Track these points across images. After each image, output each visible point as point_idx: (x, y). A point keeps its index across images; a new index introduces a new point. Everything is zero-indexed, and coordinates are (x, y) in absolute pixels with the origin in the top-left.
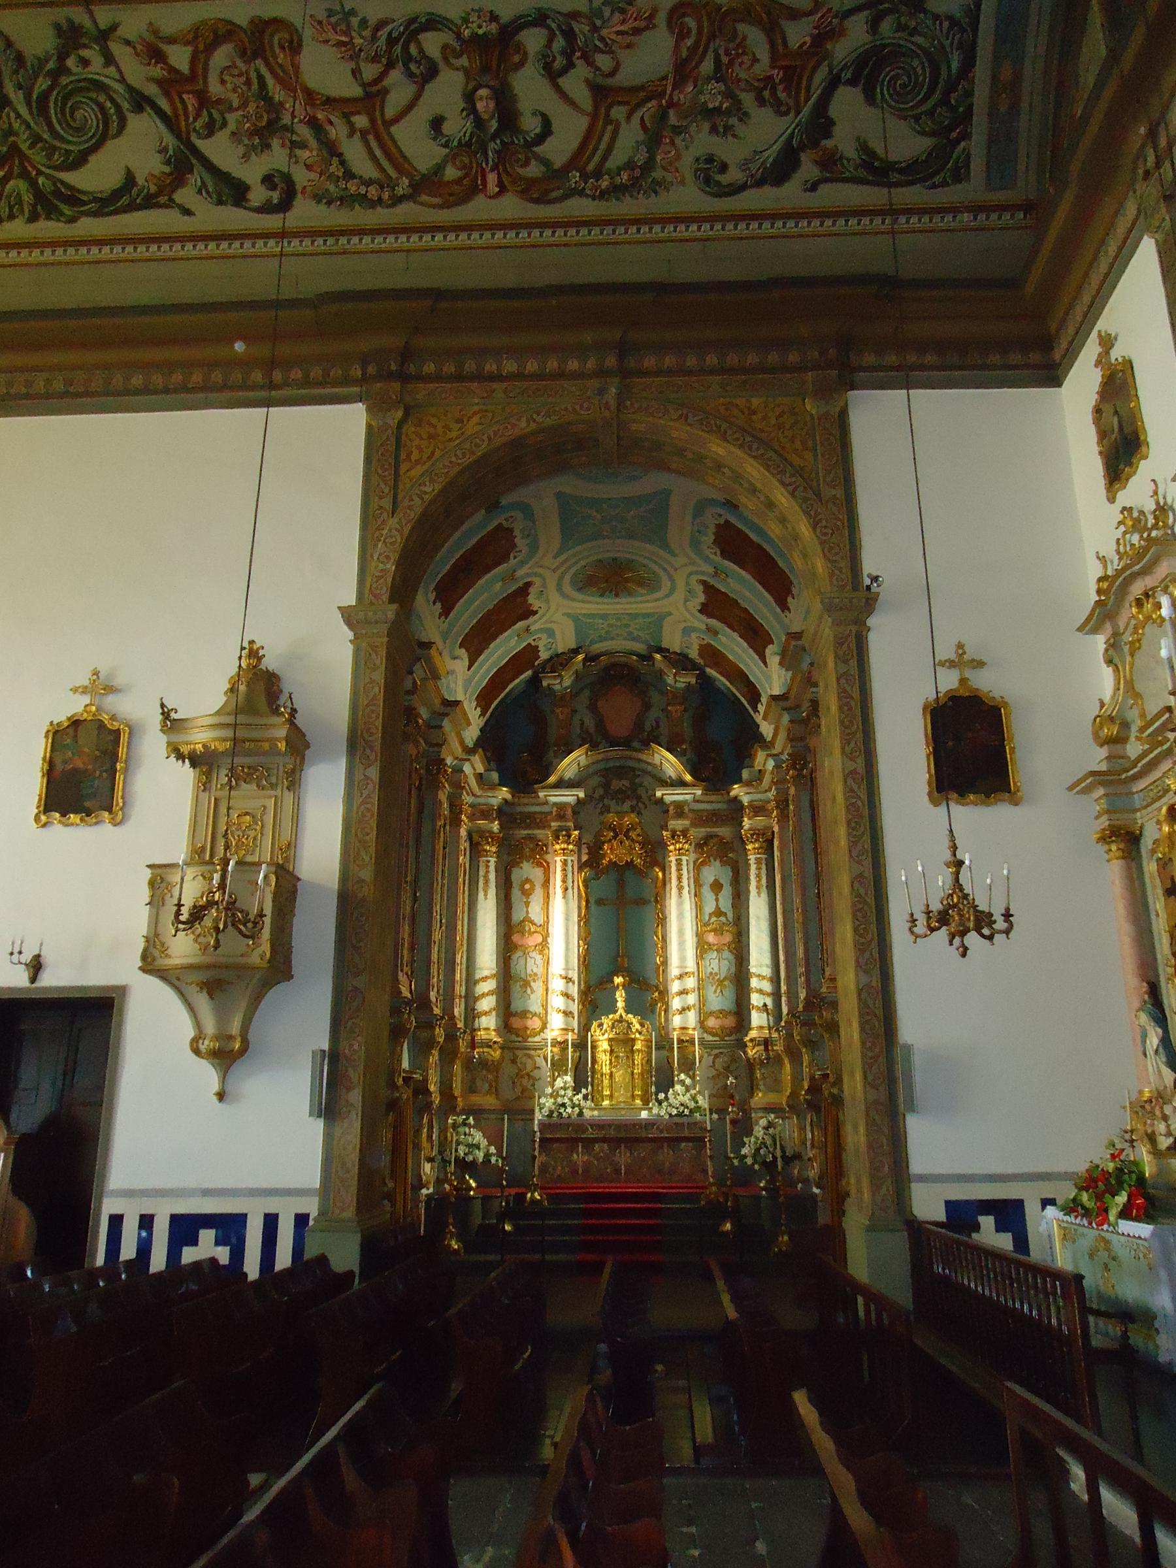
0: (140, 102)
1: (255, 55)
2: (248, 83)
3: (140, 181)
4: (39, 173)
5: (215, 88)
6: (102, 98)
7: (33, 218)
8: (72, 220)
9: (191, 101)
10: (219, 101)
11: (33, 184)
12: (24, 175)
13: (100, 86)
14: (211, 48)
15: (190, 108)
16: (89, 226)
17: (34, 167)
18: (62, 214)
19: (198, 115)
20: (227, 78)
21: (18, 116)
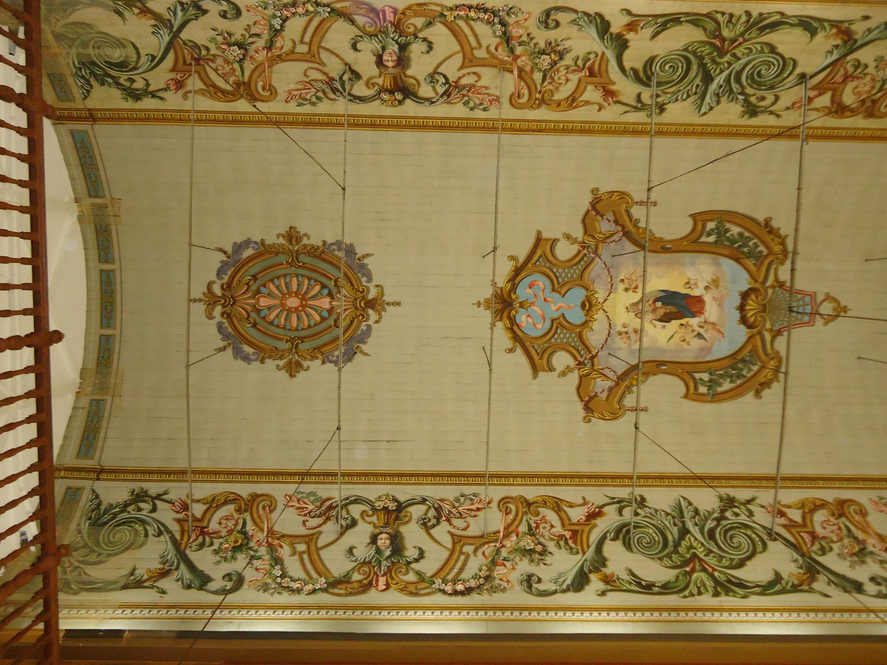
0: (773, 536)
1: (840, 516)
2: (840, 529)
3: (785, 575)
4: (714, 570)
5: (819, 531)
6: (749, 532)
7: (716, 594)
8: (745, 597)
9: (807, 537)
10: (824, 538)
11: (712, 576)
12: (704, 570)
13: (746, 526)
14: (812, 511)
15: (807, 540)
16: (755, 601)
17: (710, 566)
18: (734, 592)
19: (813, 544)
20: (825, 525)
21: (696, 539)
